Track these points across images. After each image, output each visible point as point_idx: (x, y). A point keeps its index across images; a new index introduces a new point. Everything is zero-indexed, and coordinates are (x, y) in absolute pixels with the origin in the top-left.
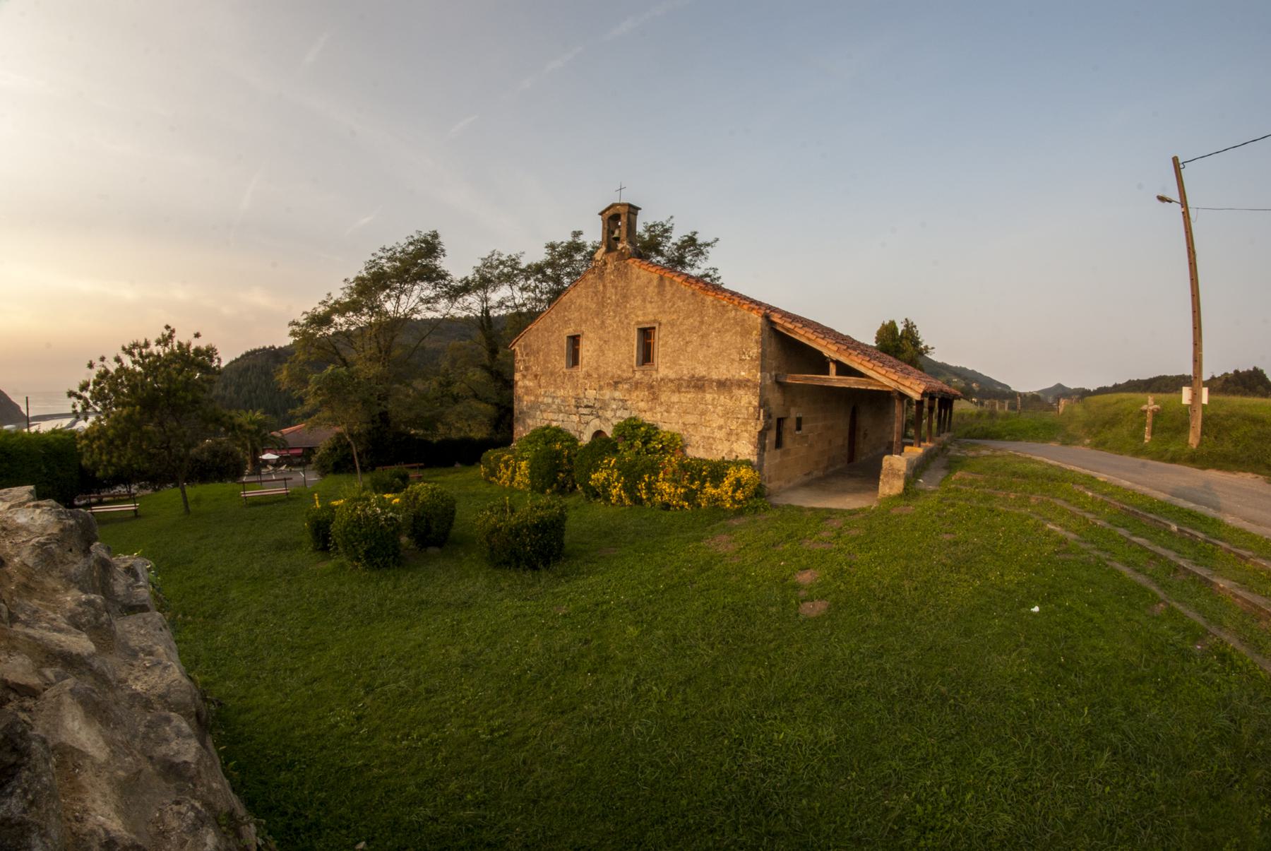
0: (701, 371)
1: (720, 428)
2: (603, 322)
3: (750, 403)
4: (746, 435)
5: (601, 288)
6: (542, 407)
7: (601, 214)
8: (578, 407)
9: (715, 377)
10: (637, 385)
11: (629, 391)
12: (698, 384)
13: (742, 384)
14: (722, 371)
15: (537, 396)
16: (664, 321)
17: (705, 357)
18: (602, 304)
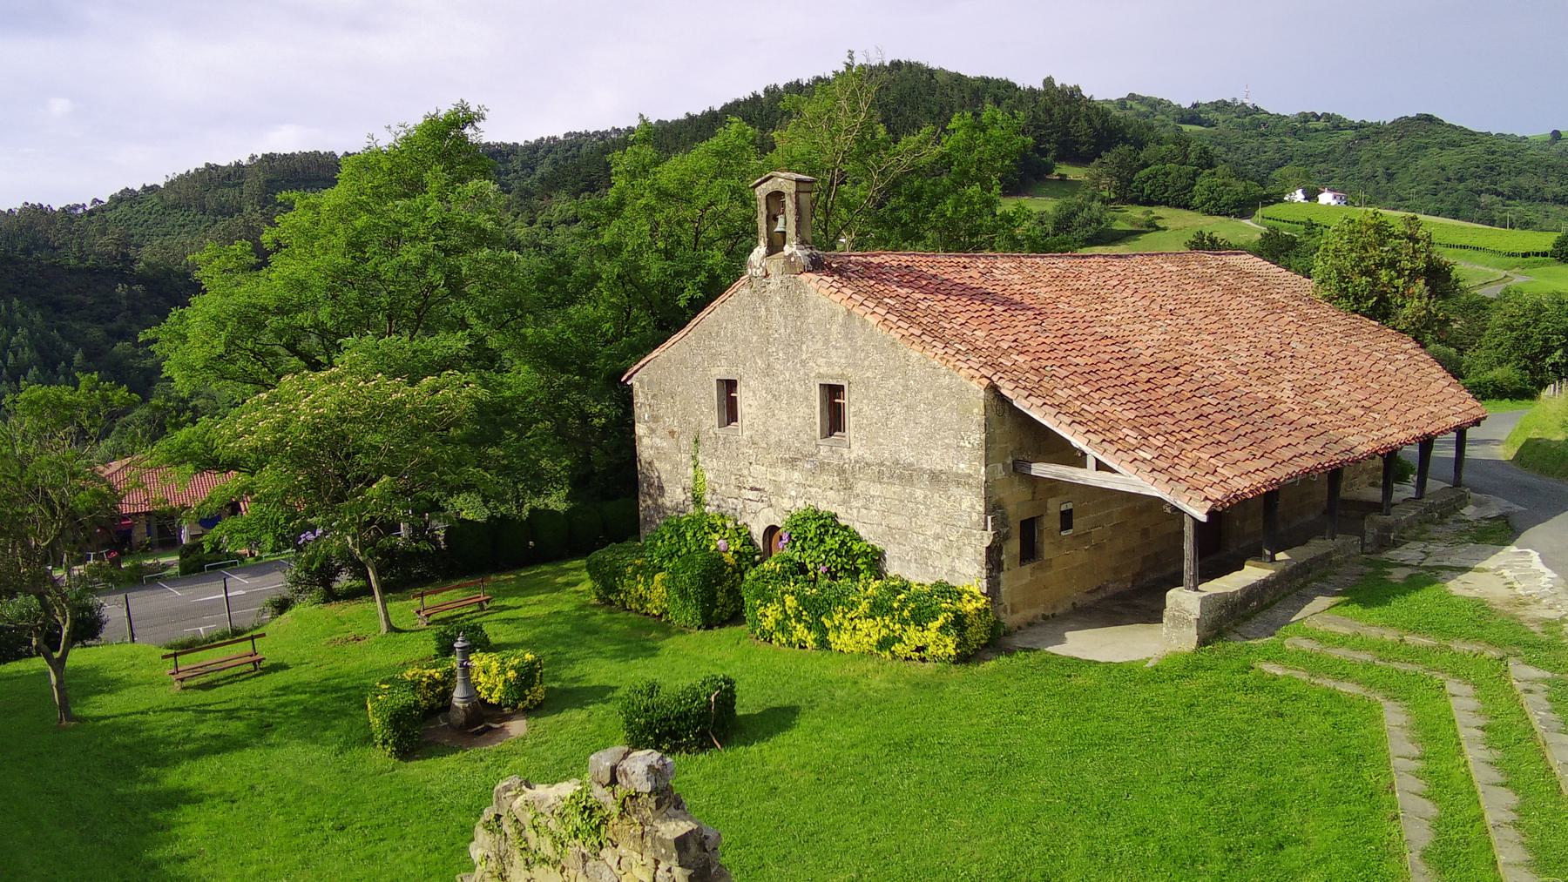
0: (907, 456)
1: (937, 537)
3: (973, 507)
5: (763, 312)
10: (822, 467)
12: (905, 474)
13: (960, 480)
14: (936, 460)
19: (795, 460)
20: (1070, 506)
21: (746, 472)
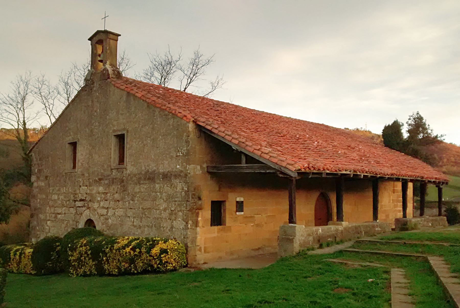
0: (152, 167)
1: (165, 210)
2: (92, 131)
3: (183, 189)
4: (180, 214)
5: (90, 103)
6: (51, 203)
7: (89, 40)
8: (75, 201)
9: (161, 171)
10: (113, 181)
12: (151, 177)
19: (100, 179)
20: (242, 199)
21: (78, 192)
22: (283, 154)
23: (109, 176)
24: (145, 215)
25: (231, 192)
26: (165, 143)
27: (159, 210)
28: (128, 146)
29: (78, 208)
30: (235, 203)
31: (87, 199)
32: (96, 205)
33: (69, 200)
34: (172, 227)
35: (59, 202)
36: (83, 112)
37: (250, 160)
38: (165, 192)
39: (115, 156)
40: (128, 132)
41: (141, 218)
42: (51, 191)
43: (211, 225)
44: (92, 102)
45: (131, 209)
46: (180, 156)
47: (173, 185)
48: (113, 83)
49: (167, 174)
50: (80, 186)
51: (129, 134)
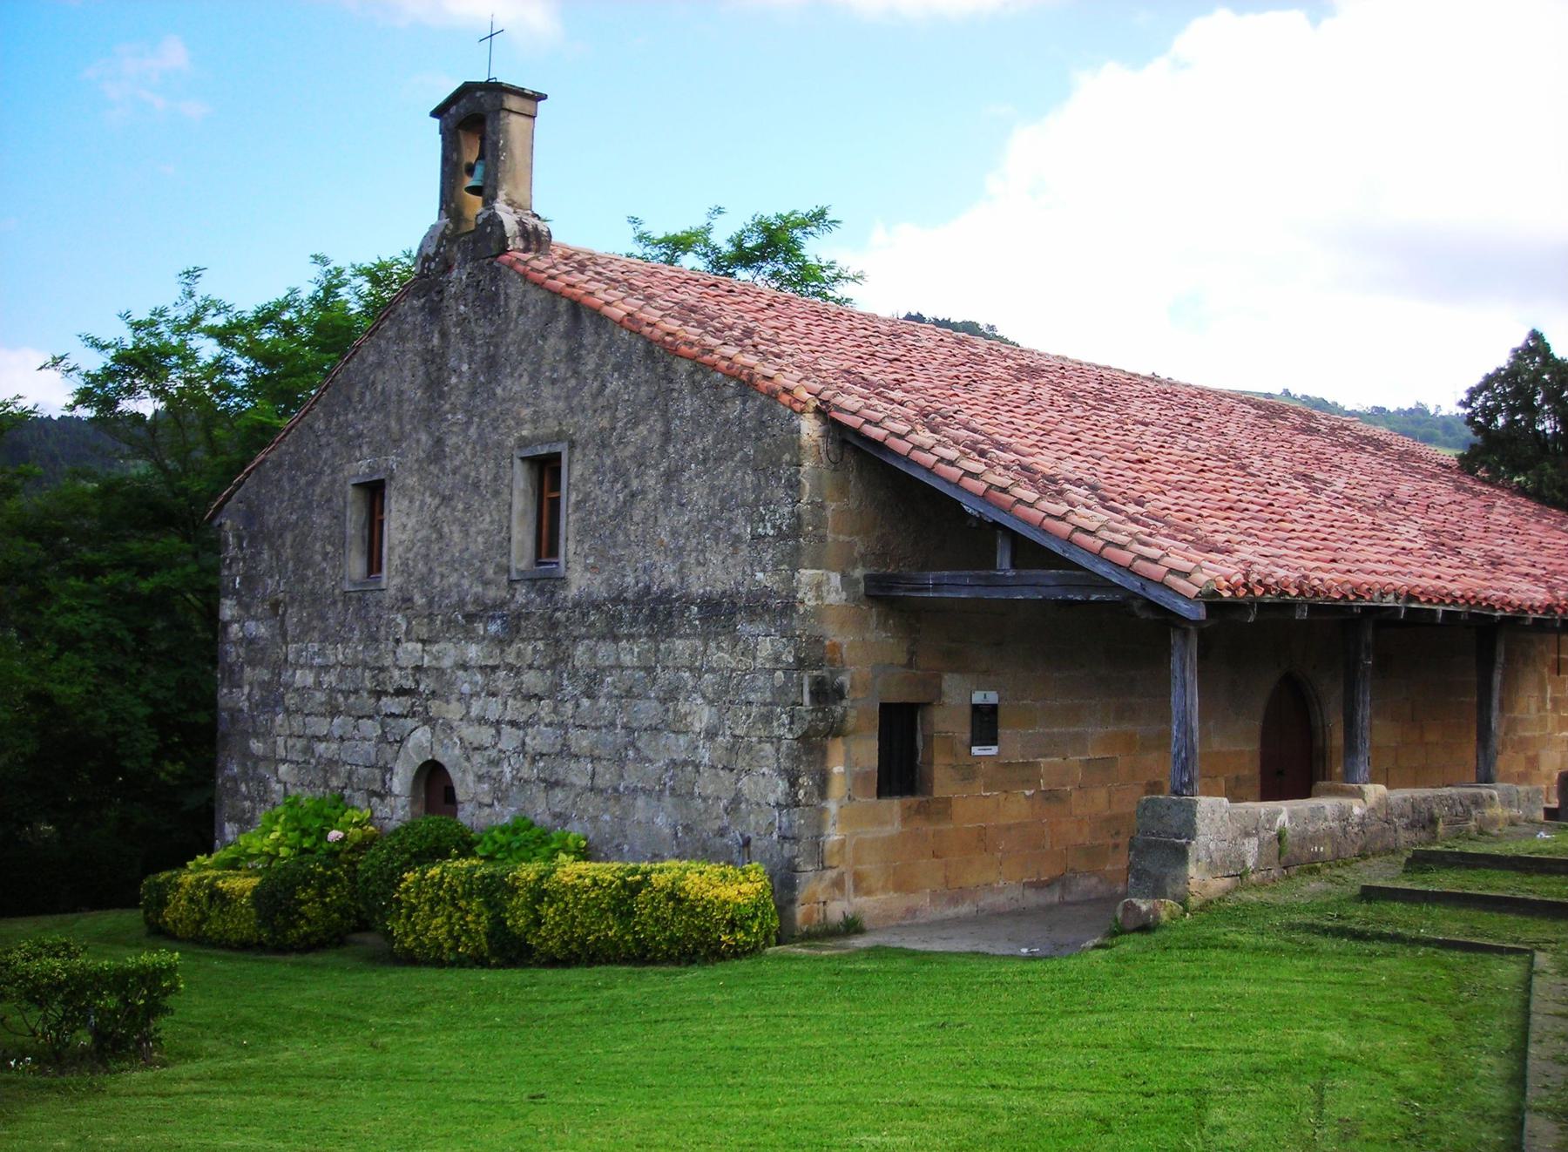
0: (667, 576)
1: (711, 734)
2: (439, 442)
3: (777, 659)
6: (291, 700)
7: (436, 113)
8: (378, 694)
9: (696, 589)
11: (501, 642)
12: (658, 612)
14: (714, 573)
15: (279, 666)
16: (581, 437)
17: (674, 533)
18: (435, 386)
19: (470, 618)
20: (992, 698)
22: (1150, 535)
23: (504, 603)
24: (638, 750)
25: (952, 671)
26: (712, 488)
27: (686, 733)
28: (573, 498)
29: (388, 720)
30: (968, 711)
31: (422, 687)
32: (454, 711)
33: (356, 692)
34: (736, 800)
35: (320, 696)
36: (407, 372)
37: (1032, 552)
38: (712, 670)
39: (522, 536)
40: (572, 445)
41: (621, 761)
42: (290, 657)
43: (880, 795)
44: (444, 335)
45: (585, 727)
46: (766, 535)
47: (741, 645)
48: (520, 267)
49: (719, 604)
50: (398, 641)
51: (578, 454)
